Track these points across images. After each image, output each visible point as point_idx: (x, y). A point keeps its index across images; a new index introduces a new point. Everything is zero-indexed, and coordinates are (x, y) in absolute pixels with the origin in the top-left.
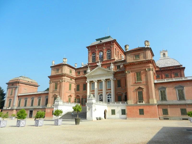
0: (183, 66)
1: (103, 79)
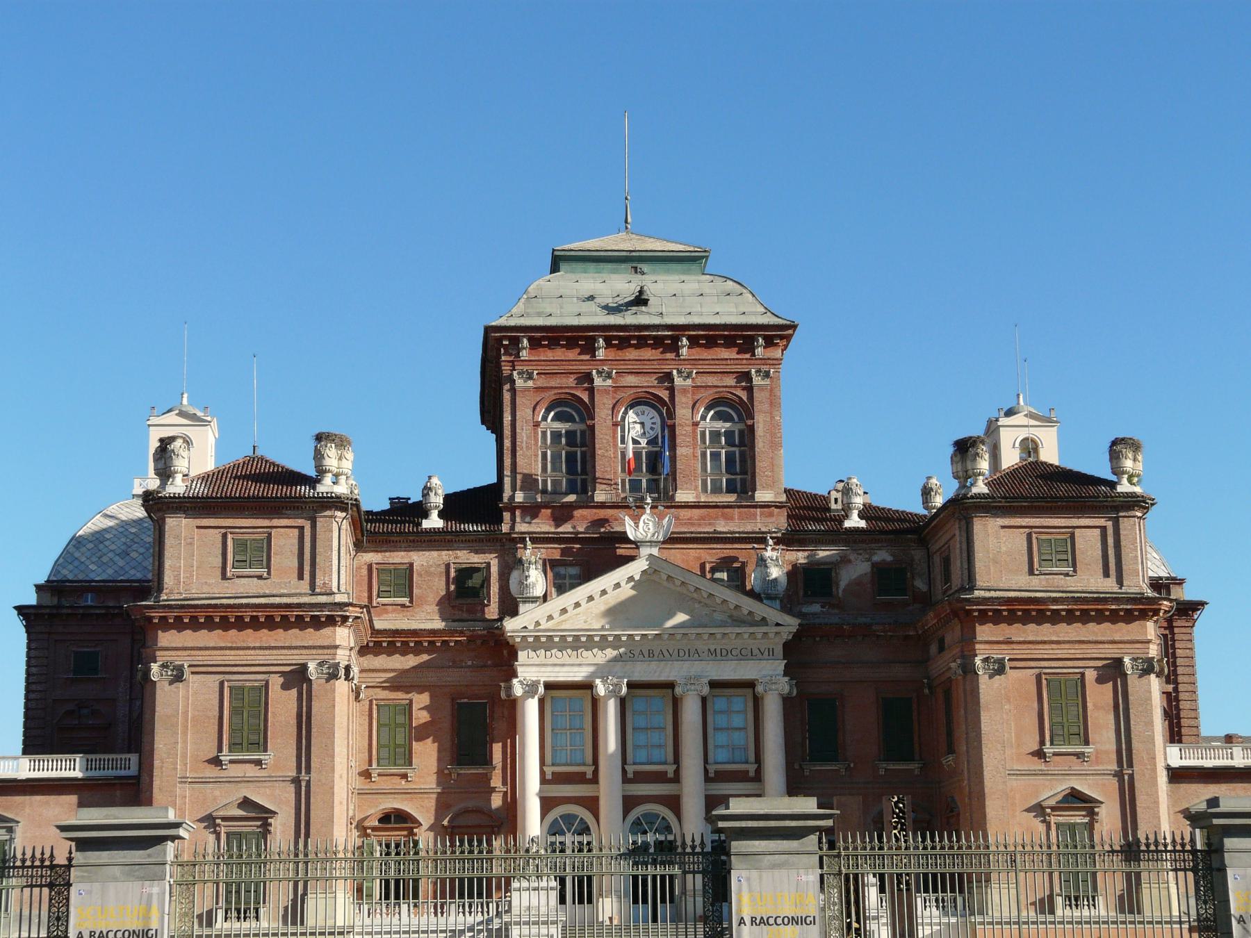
0: (1187, 593)
1: (693, 675)
